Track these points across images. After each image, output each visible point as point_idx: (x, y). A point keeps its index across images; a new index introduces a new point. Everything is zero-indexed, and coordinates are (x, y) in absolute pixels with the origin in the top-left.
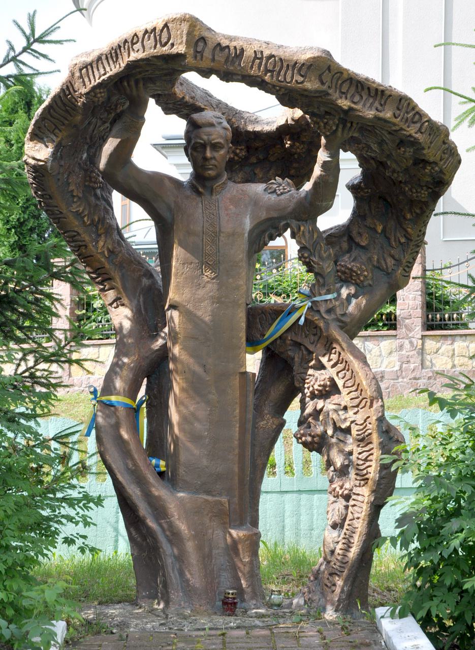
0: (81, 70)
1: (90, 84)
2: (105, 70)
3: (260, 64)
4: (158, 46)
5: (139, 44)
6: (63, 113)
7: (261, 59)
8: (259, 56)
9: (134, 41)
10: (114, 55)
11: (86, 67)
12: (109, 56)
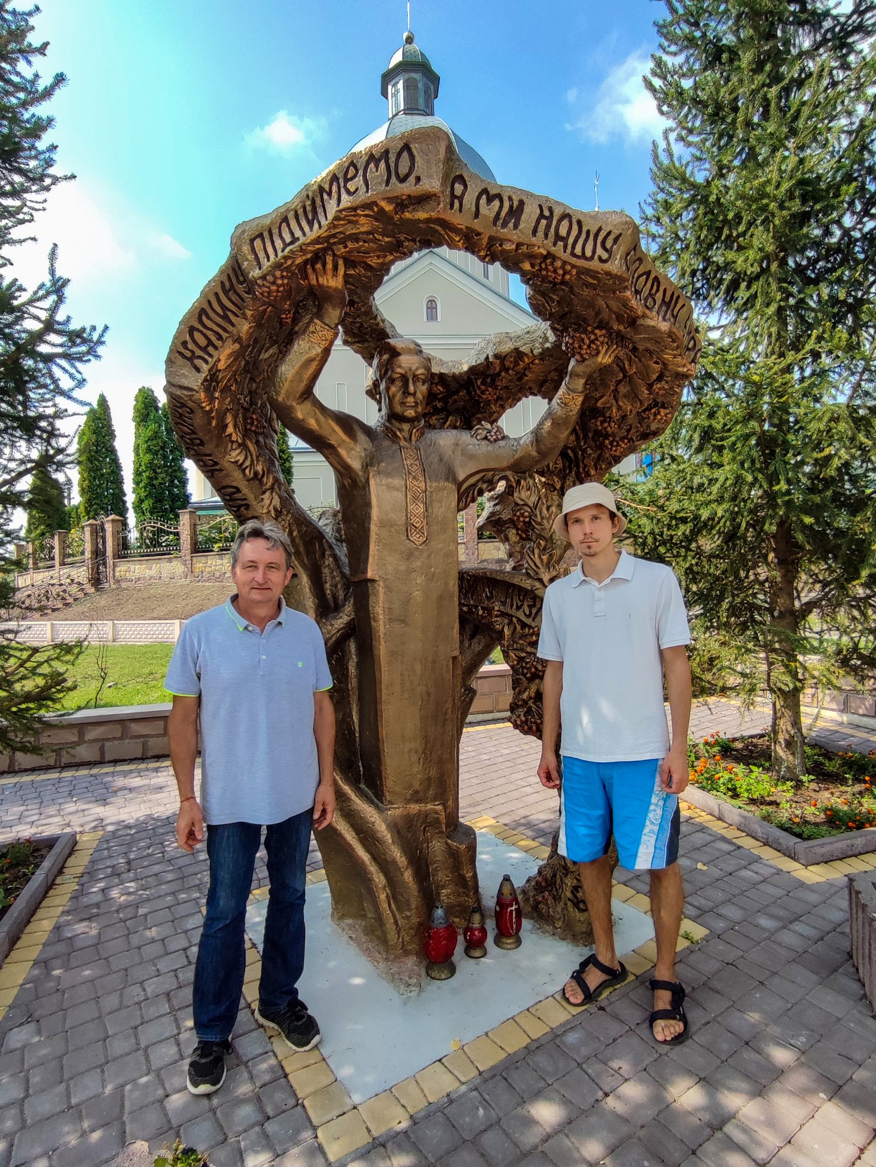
1: (268, 260)
2: (292, 234)
3: (548, 227)
7: (550, 218)
8: (547, 213)
11: (261, 236)
12: (300, 212)
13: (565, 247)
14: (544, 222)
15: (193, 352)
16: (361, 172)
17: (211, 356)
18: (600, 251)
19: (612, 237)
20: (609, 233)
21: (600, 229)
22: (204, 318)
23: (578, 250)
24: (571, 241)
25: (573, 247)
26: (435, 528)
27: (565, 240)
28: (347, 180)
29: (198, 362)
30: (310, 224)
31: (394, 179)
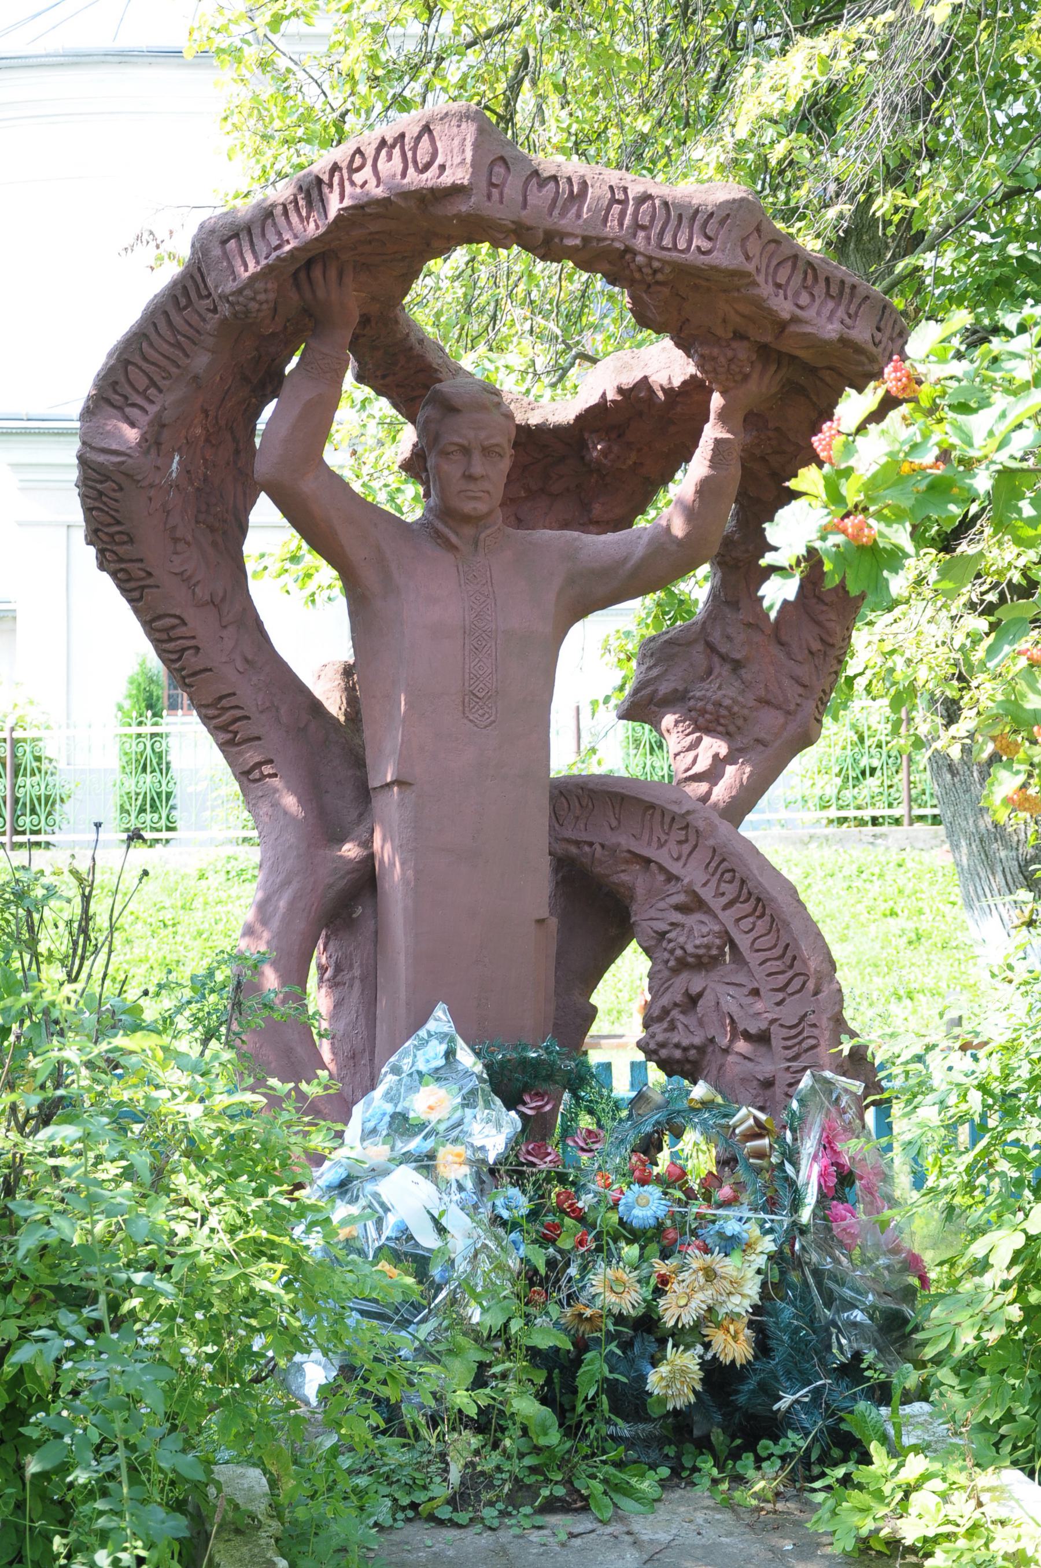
3: (622, 214)
7: (624, 202)
9: (355, 165)
16: (369, 162)
22: (144, 345)
23: (667, 241)
25: (661, 235)
31: (411, 170)
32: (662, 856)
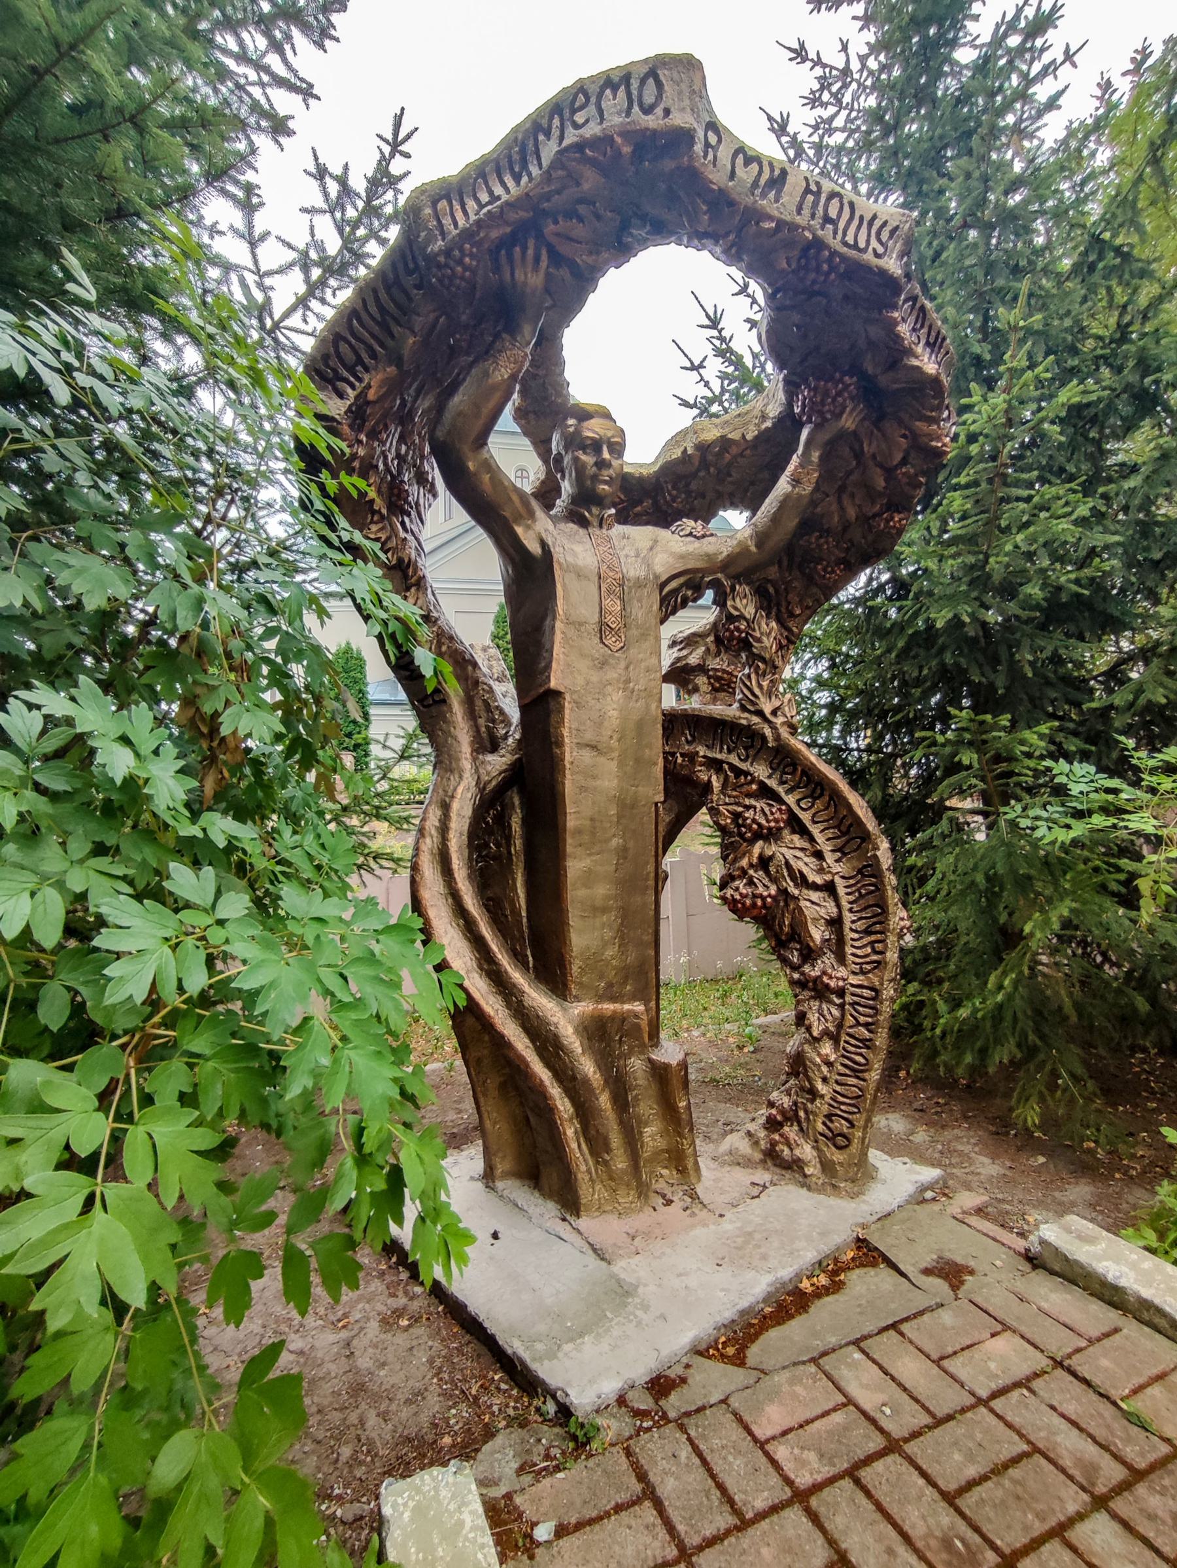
0: (434, 204)
2: (491, 193)
3: (815, 204)
4: (636, 108)
5: (592, 109)
6: (376, 329)
7: (818, 194)
8: (814, 188)
9: (577, 104)
10: (516, 157)
13: (835, 232)
14: (810, 198)
15: (334, 370)
17: (360, 380)
18: (874, 243)
19: (888, 228)
20: (885, 223)
21: (874, 217)
24: (842, 225)
25: (845, 234)
26: (634, 632)
27: (834, 222)
28: (574, 111)
29: (342, 385)
30: (517, 178)
32: (734, 759)
